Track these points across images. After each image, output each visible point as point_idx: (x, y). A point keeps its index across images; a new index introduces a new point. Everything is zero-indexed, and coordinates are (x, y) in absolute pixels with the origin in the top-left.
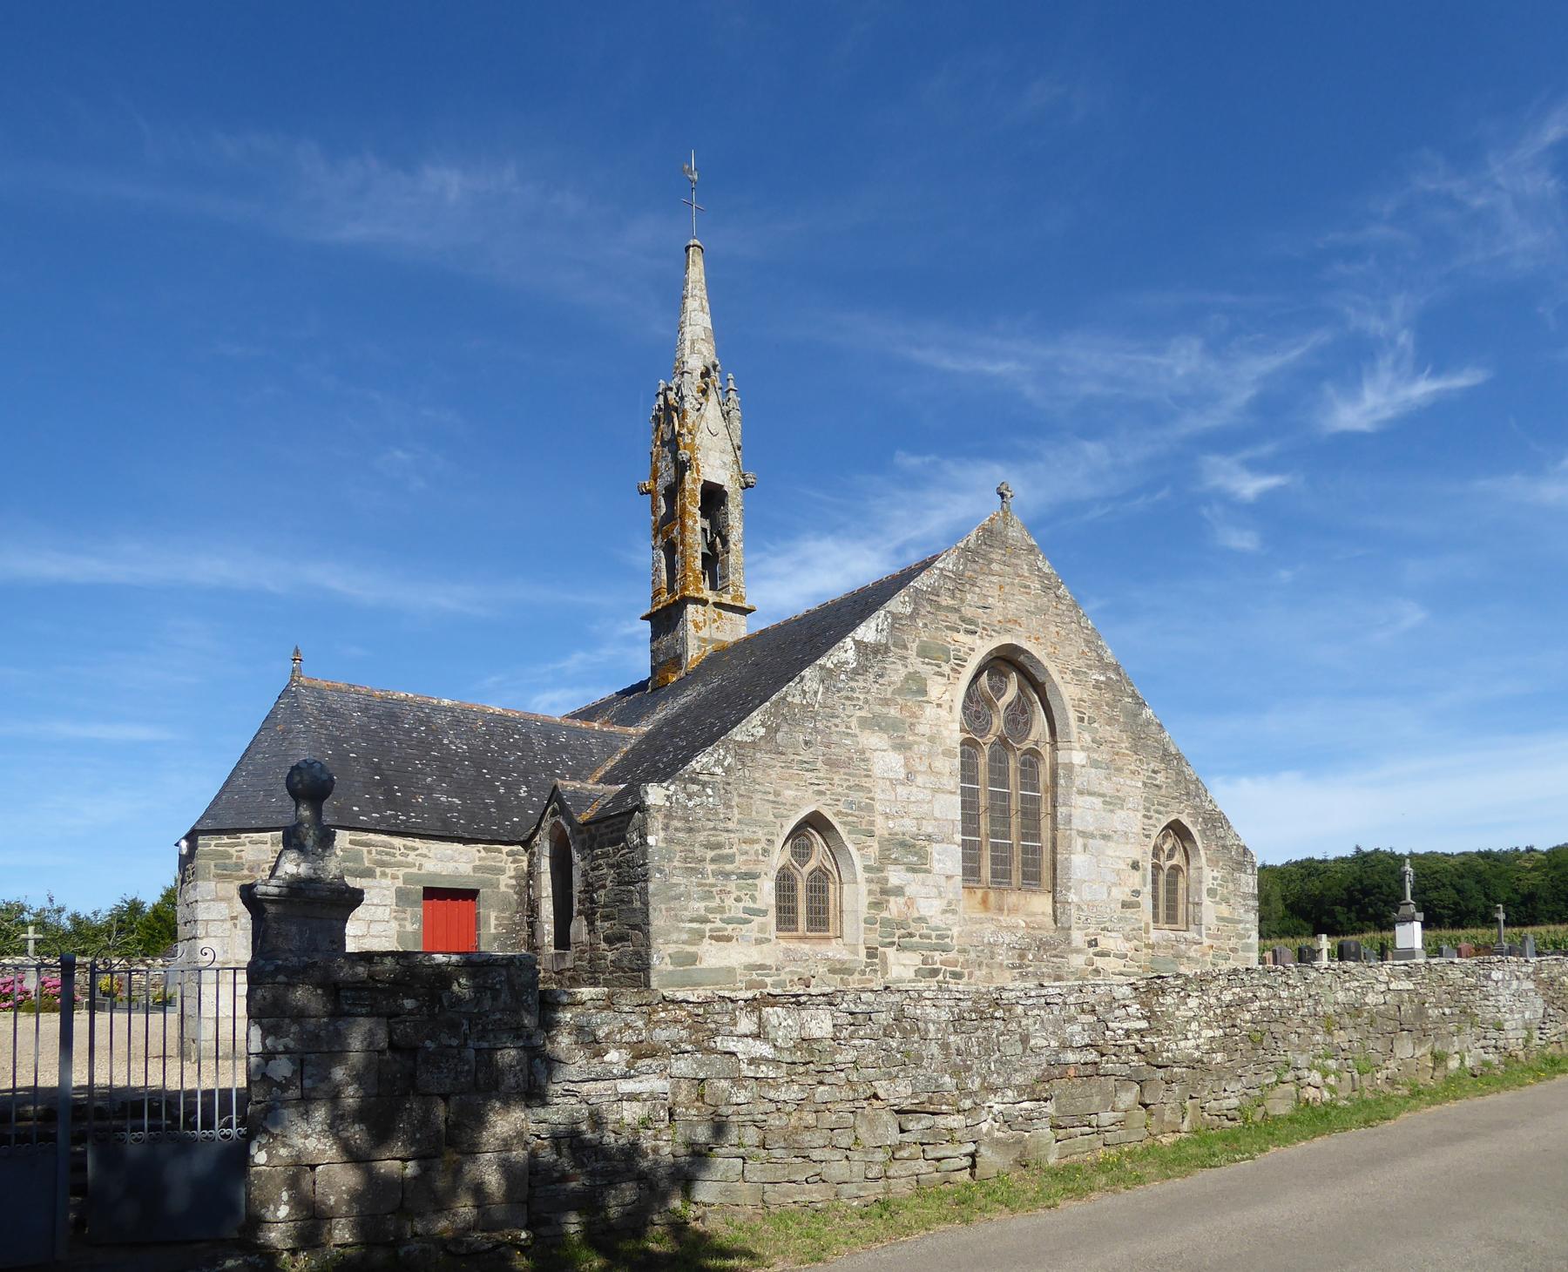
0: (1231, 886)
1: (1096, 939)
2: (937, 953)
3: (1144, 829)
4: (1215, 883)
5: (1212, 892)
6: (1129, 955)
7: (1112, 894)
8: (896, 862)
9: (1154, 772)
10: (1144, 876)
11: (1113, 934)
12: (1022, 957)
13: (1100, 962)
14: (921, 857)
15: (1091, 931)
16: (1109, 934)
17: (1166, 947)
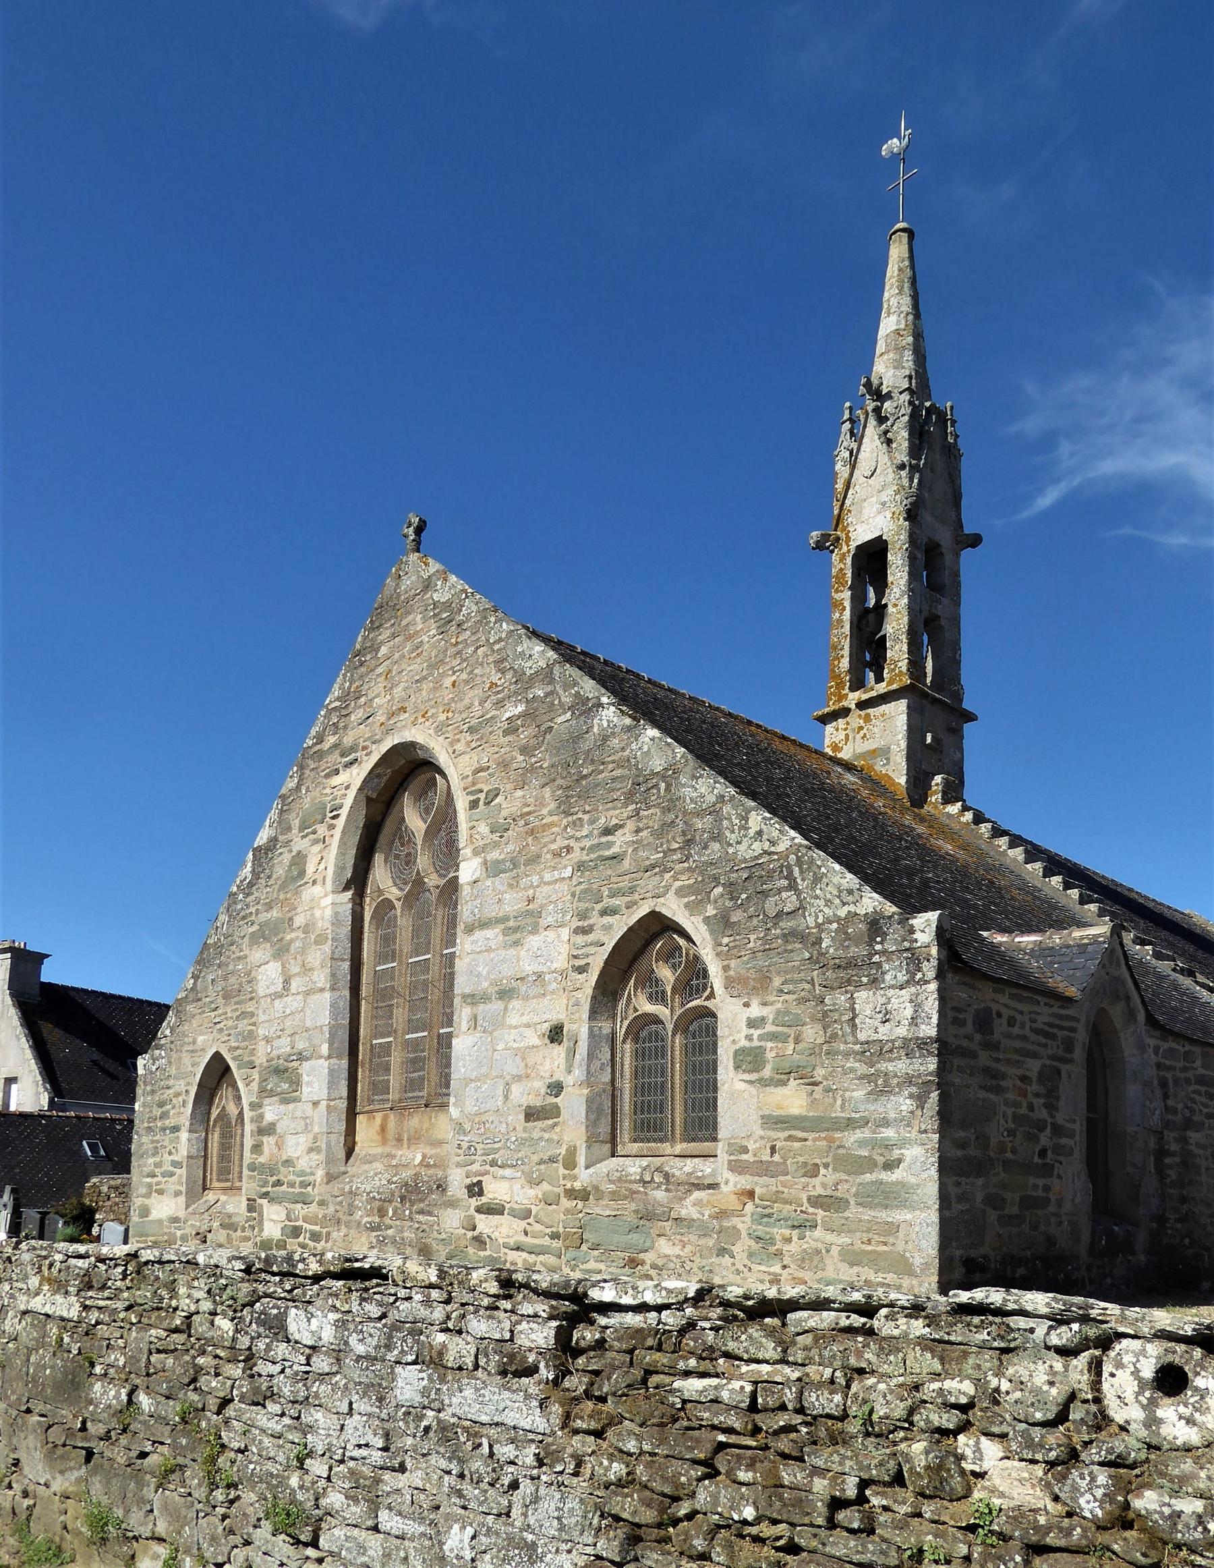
0: (812, 1033)
1: (479, 1183)
2: (299, 1206)
3: (575, 957)
4: (756, 1033)
5: (749, 1059)
6: (534, 1210)
7: (512, 1097)
8: (271, 1094)
9: (607, 831)
10: (572, 1053)
11: (508, 1172)
12: (382, 1212)
13: (485, 1224)
14: (291, 1083)
15: (475, 1167)
16: (501, 1172)
17: (615, 1196)
